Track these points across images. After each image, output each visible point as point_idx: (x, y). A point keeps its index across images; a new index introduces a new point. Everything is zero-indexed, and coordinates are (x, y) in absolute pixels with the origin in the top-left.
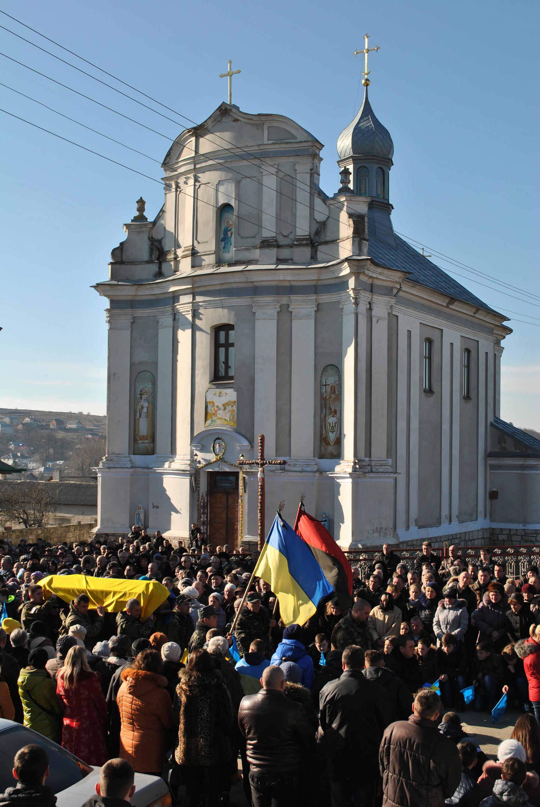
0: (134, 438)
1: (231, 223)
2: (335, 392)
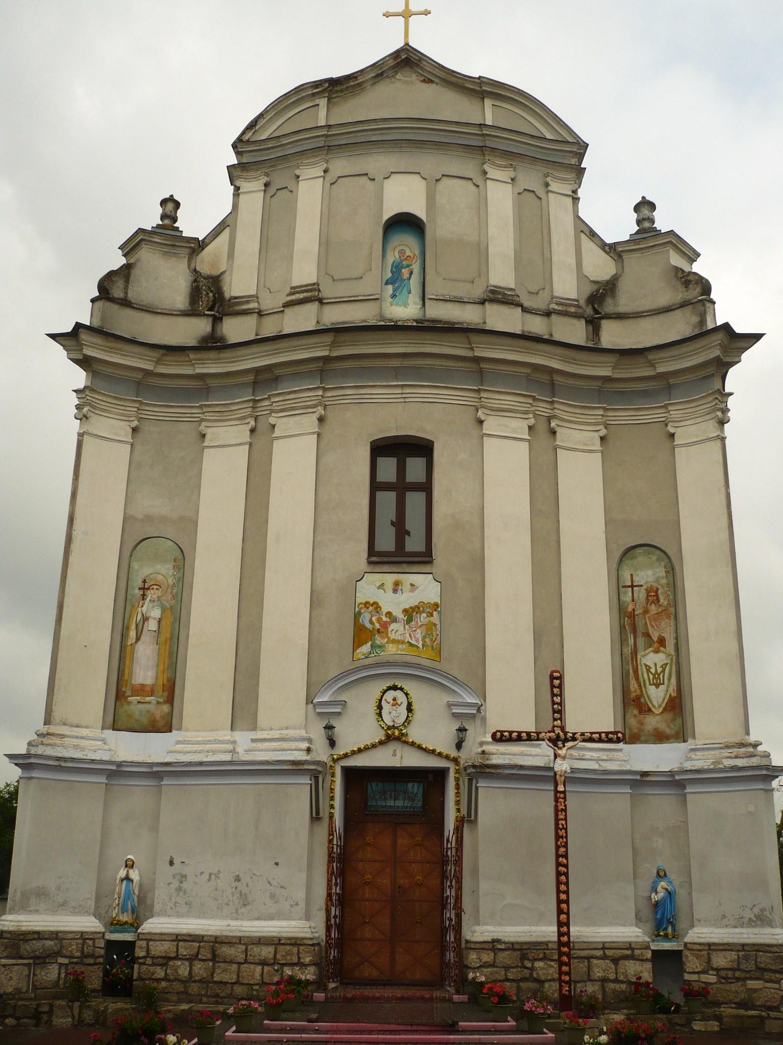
0: (120, 689)
1: (408, 253)
2: (658, 600)
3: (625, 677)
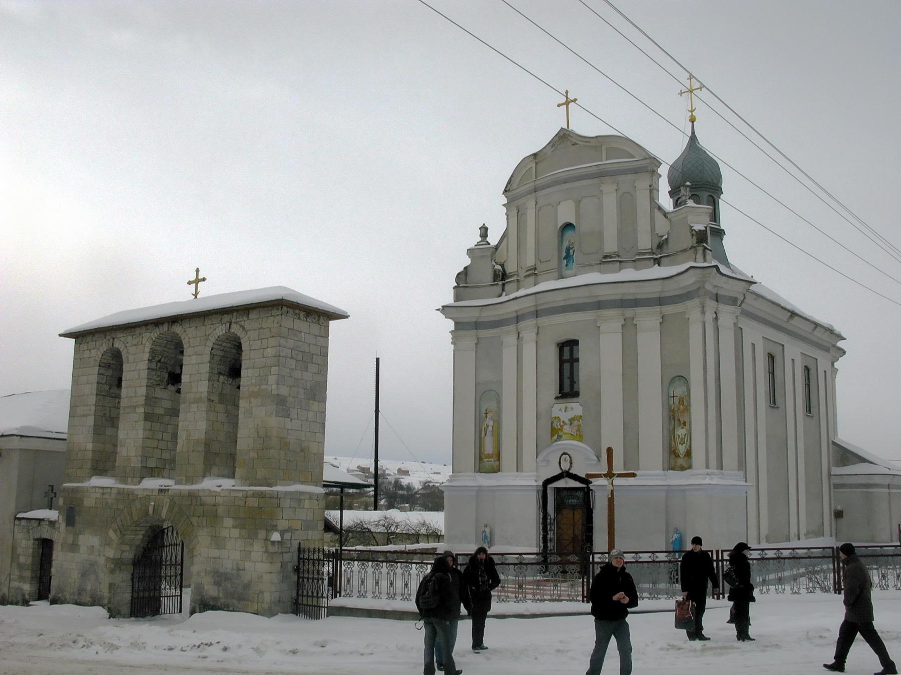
0: (480, 457)
3: (670, 440)
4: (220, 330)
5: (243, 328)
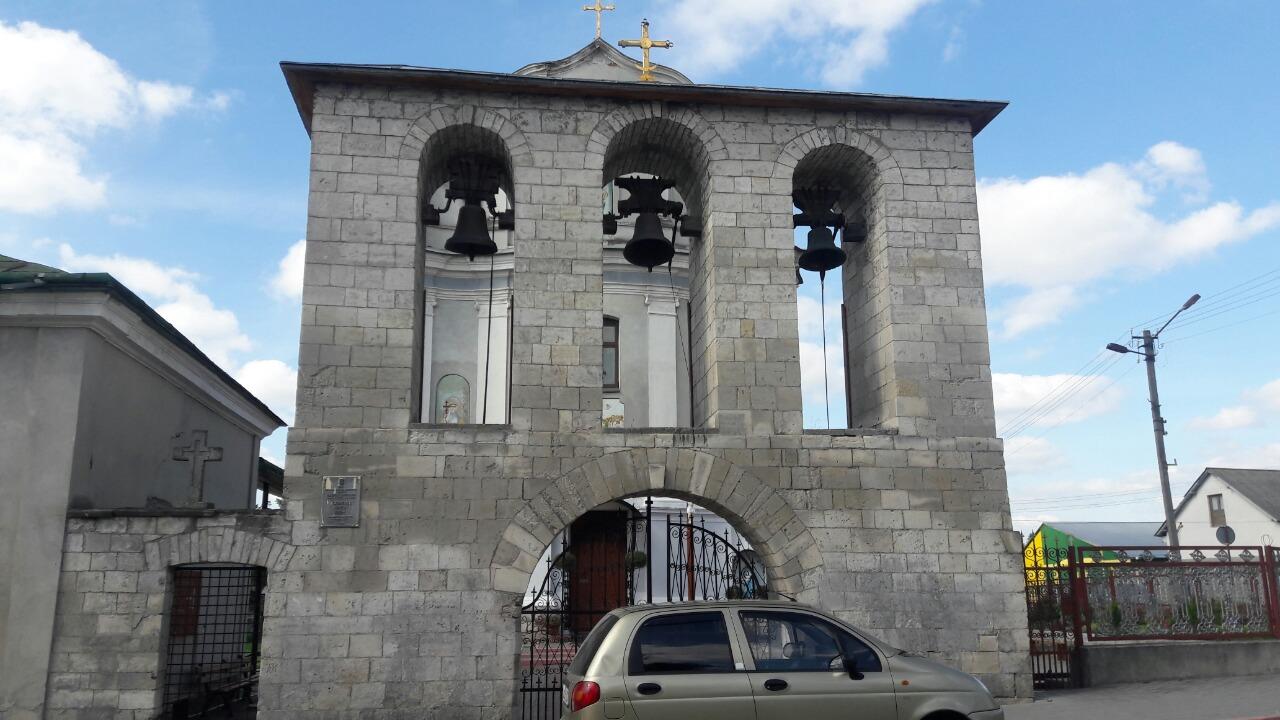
4: (815, 137)
5: (879, 142)
